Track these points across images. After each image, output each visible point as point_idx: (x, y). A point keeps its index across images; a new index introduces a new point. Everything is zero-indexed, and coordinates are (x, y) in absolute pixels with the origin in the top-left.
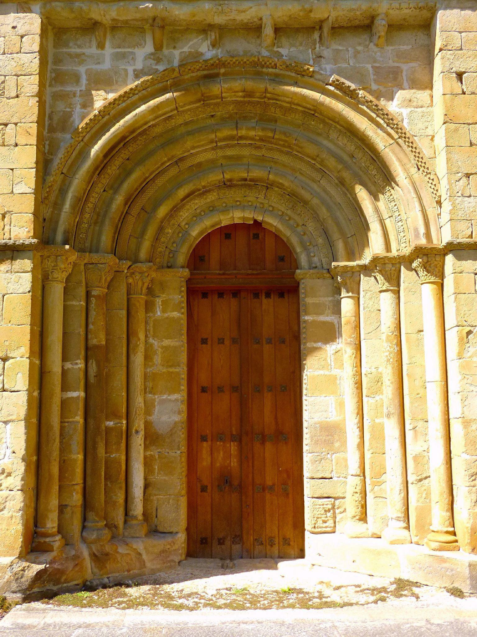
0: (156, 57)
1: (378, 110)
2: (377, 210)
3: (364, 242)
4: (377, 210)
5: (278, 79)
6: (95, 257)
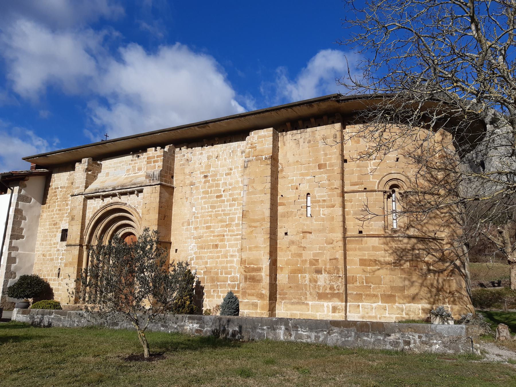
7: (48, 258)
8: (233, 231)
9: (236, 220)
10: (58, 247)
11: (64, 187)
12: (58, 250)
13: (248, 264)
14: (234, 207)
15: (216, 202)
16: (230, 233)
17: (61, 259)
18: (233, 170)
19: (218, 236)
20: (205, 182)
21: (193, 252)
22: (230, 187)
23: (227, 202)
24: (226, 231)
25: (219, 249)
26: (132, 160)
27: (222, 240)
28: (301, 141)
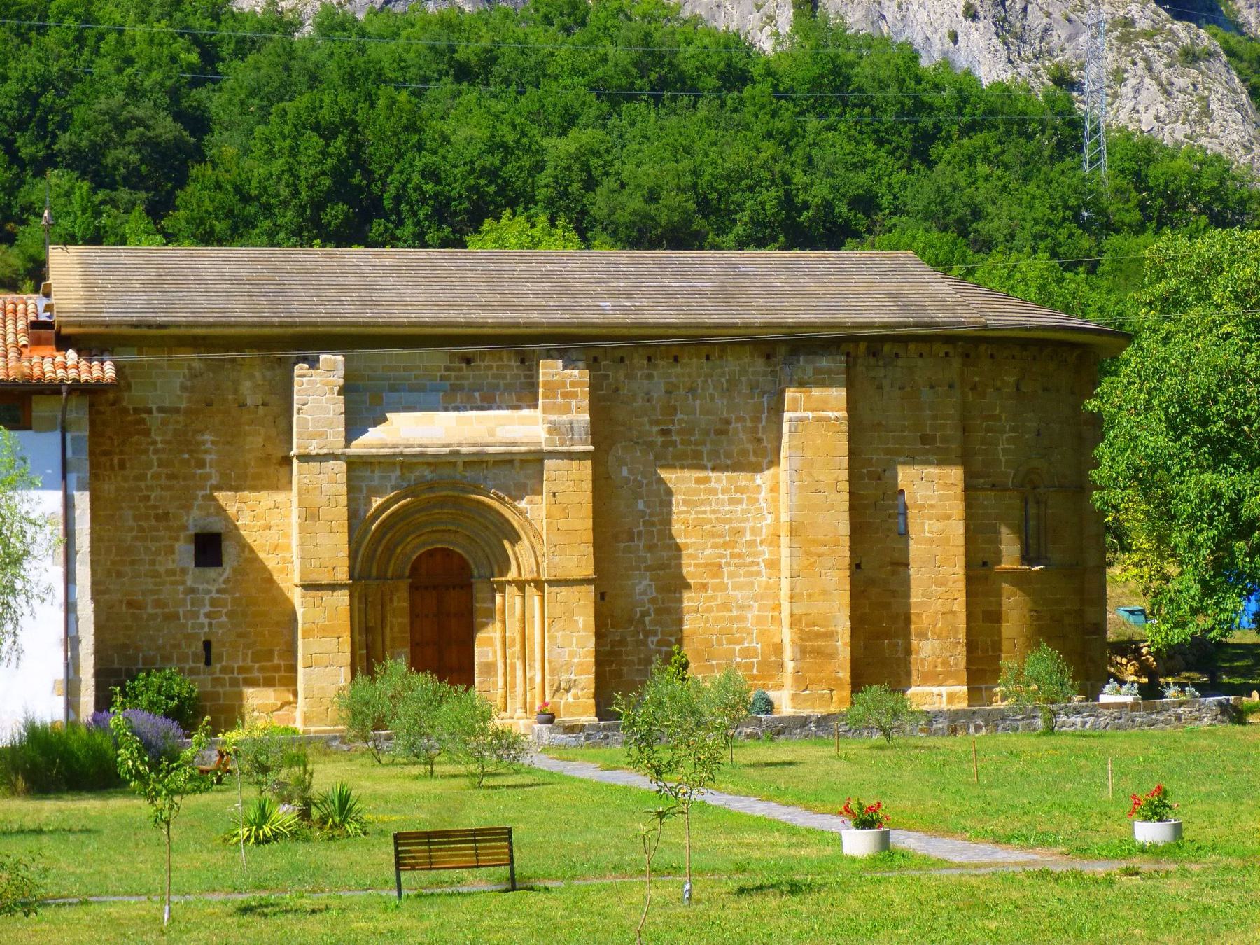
0: (402, 477)
1: (514, 507)
2: (515, 554)
3: (508, 568)
4: (515, 554)
5: (464, 490)
6: (369, 582)
7: (150, 611)
8: (740, 556)
9: (748, 533)
10: (189, 583)
11: (177, 410)
12: (193, 591)
13: (807, 625)
14: (740, 507)
15: (696, 492)
16: (736, 561)
17: (207, 615)
18: (733, 425)
19: (706, 565)
20: (665, 445)
21: (646, 598)
22: (729, 462)
23: (723, 493)
24: (724, 556)
25: (710, 593)
26: (447, 369)
27: (715, 576)
28: (886, 383)
